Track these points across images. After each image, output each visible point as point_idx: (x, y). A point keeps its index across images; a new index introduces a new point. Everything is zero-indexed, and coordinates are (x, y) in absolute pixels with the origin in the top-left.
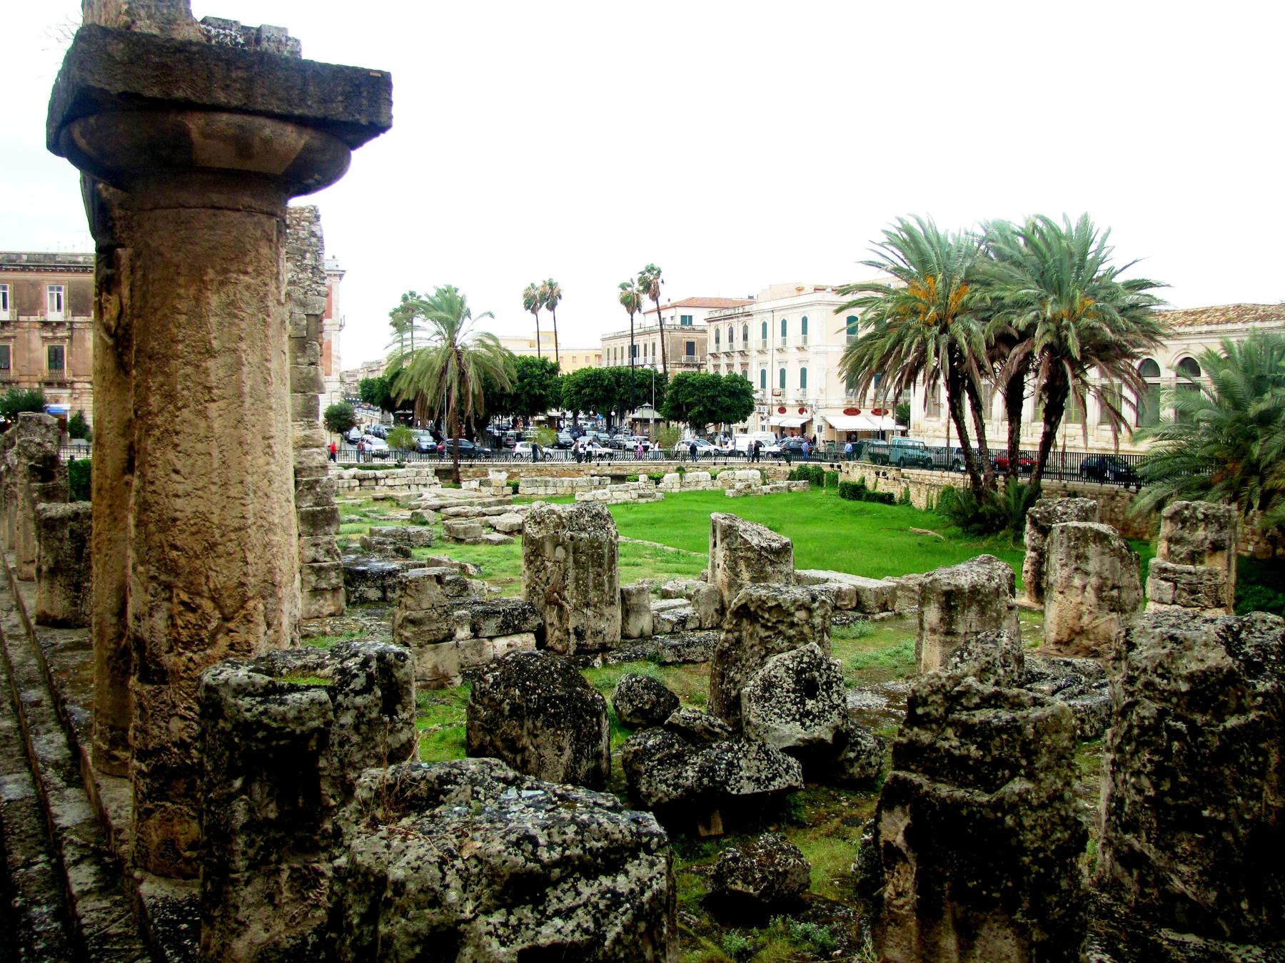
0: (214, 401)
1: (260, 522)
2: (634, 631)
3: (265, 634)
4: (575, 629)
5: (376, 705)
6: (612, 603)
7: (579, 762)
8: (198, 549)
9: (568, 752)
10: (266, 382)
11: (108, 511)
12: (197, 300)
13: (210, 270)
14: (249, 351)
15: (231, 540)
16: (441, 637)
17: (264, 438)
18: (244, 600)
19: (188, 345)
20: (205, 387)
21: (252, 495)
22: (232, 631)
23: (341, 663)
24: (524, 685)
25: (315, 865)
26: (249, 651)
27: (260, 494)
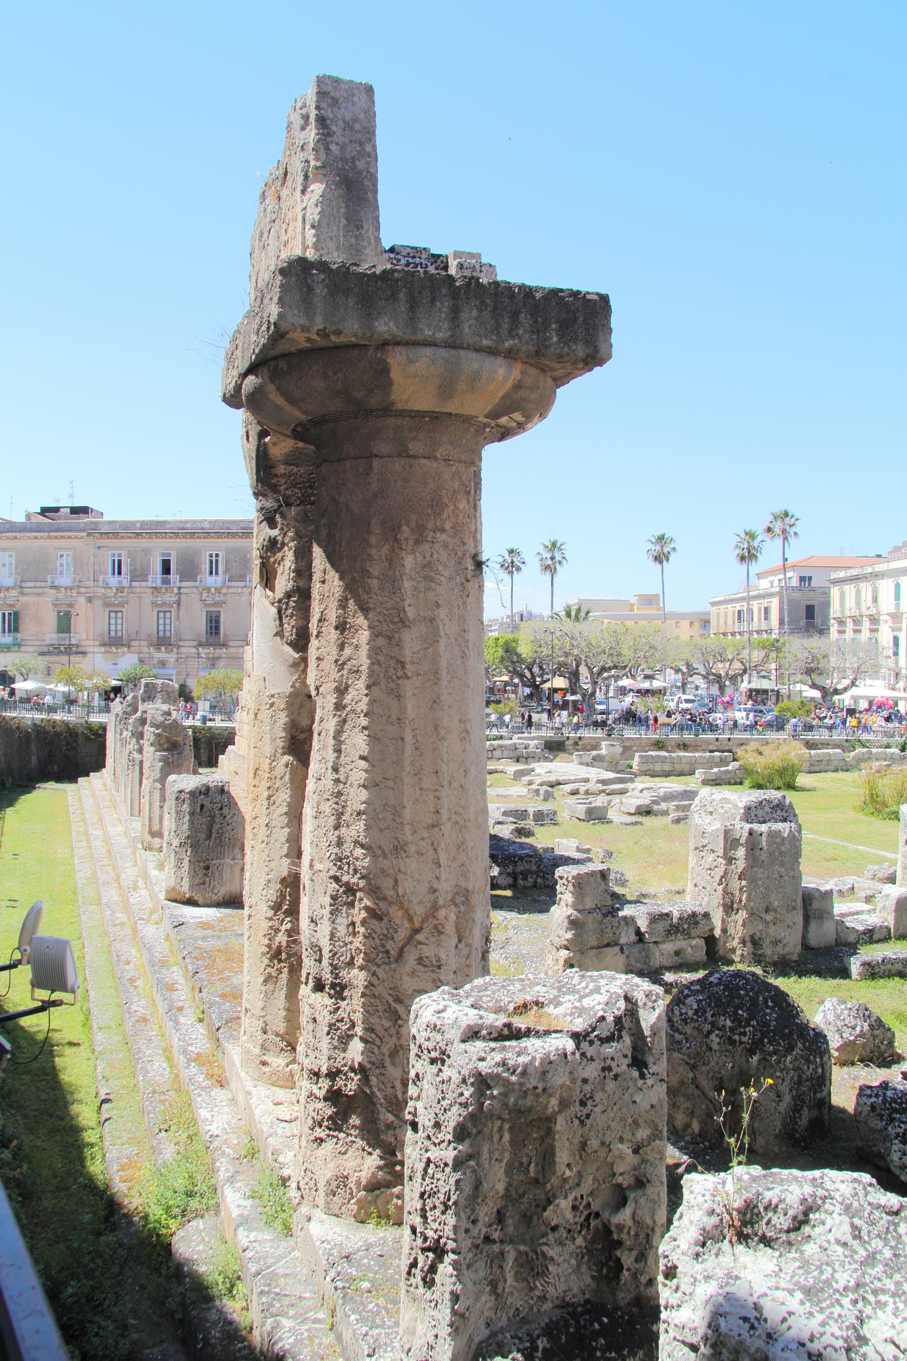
0: (407, 678)
1: (454, 818)
2: (814, 940)
3: (456, 946)
4: (752, 937)
5: (625, 1056)
6: (794, 908)
7: (799, 1111)
8: (387, 848)
9: (787, 1098)
10: (464, 656)
11: (266, 794)
12: (390, 561)
13: (404, 528)
14: (447, 621)
15: (423, 839)
16: (605, 942)
17: (460, 721)
18: (435, 907)
19: (379, 614)
20: (398, 661)
21: (446, 787)
22: (420, 943)
23: (580, 1000)
24: (736, 1013)
25: (545, 1248)
26: (439, 967)
27: (456, 785)
